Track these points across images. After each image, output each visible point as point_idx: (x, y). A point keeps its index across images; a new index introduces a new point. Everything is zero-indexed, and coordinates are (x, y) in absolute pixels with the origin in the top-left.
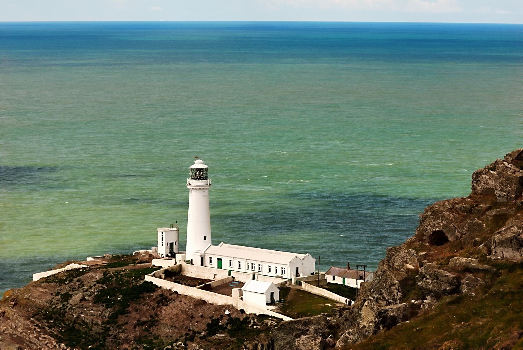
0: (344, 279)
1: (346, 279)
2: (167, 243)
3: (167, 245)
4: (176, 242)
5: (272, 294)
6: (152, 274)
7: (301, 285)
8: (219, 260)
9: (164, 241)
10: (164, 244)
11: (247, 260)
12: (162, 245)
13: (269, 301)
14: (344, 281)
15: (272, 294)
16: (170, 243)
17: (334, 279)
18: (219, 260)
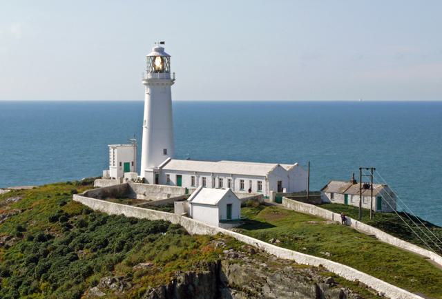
0: (346, 196)
1: (349, 196)
2: (121, 163)
3: (121, 165)
4: (133, 163)
5: (229, 206)
6: (84, 192)
7: (281, 203)
8: (179, 178)
9: (116, 160)
10: (116, 163)
11: (213, 173)
12: (114, 165)
13: (225, 218)
14: (346, 200)
15: (229, 206)
16: (125, 163)
17: (332, 197)
18: (179, 178)
